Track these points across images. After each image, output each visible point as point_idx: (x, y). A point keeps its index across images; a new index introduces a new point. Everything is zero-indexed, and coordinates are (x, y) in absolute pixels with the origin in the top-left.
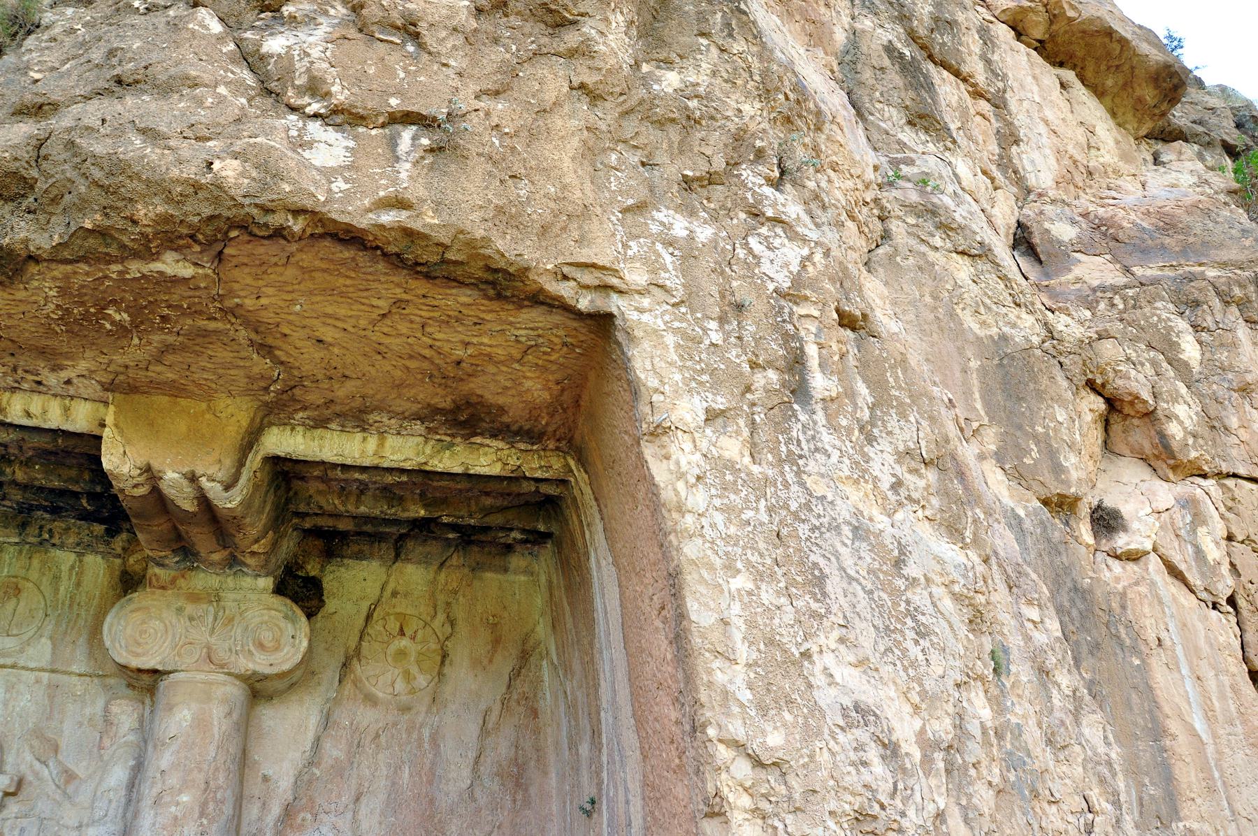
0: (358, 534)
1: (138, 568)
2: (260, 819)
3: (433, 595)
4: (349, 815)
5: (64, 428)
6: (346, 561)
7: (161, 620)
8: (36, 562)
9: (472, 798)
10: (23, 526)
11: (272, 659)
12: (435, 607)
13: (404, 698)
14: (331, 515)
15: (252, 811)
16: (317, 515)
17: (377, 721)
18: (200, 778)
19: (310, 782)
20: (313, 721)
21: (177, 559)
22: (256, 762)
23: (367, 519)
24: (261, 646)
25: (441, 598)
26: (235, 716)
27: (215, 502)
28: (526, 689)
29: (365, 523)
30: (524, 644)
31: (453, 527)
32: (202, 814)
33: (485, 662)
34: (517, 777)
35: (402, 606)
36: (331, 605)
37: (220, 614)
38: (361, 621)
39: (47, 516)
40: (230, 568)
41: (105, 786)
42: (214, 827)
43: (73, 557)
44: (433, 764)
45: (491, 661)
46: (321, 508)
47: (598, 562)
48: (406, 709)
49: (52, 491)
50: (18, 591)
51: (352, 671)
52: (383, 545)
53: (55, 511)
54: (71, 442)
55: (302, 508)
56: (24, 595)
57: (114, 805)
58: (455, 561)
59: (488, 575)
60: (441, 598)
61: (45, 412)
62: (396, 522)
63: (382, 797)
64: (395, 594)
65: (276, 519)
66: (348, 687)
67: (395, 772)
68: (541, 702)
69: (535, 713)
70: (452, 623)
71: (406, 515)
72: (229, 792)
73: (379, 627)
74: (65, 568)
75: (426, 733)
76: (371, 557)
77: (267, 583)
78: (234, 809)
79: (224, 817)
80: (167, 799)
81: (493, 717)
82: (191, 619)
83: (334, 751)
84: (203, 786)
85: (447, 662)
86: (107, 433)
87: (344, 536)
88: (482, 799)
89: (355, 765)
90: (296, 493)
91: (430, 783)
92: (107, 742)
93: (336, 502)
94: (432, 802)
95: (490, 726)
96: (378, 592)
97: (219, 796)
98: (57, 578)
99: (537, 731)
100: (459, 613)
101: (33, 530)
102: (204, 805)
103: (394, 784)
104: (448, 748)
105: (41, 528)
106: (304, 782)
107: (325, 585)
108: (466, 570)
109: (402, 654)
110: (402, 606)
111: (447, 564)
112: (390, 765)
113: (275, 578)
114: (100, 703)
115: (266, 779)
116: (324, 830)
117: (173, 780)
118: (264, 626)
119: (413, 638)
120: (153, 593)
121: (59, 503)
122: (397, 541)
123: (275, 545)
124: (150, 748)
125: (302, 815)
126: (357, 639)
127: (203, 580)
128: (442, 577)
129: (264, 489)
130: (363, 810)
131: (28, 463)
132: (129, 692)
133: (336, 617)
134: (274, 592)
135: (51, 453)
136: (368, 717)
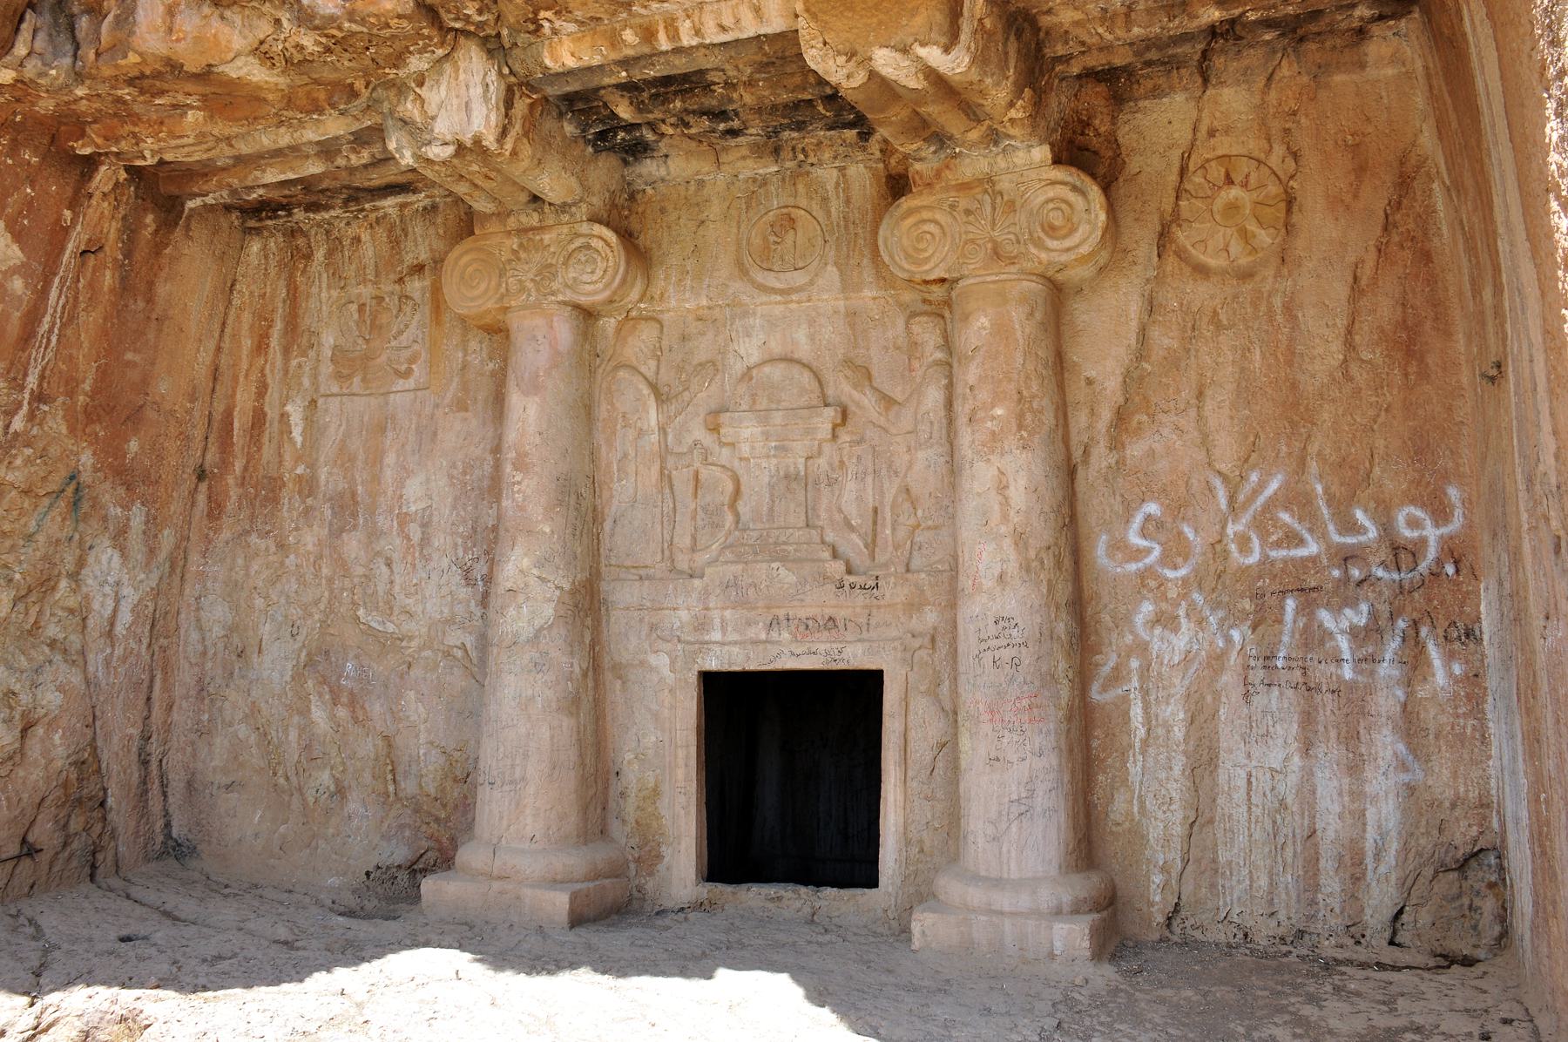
0: (1149, 64)
1: (900, 169)
2: (1090, 427)
3: (1263, 123)
4: (1193, 413)
5: (762, 32)
6: (1141, 104)
7: (936, 222)
8: (800, 187)
9: (1348, 377)
10: (777, 151)
11: (1067, 243)
13: (1244, 261)
14: (1101, 49)
15: (1079, 420)
16: (1083, 53)
18: (1011, 388)
19: (1141, 378)
20: (1135, 308)
21: (933, 149)
22: (1075, 364)
23: (1149, 43)
24: (1051, 230)
26: (1038, 316)
27: (941, 70)
28: (1411, 226)
29: (1148, 48)
30: (1402, 163)
31: (1268, 24)
32: (1020, 427)
33: (1348, 198)
34: (1408, 344)
36: (1134, 165)
37: (999, 200)
38: (1173, 178)
39: (795, 135)
40: (996, 143)
41: (923, 409)
42: (1037, 438)
43: (835, 173)
44: (1291, 339)
45: (1356, 196)
46: (1083, 43)
47: (1472, 20)
48: (1246, 275)
49: (786, 106)
50: (792, 220)
51: (1172, 241)
52: (1183, 71)
53: (800, 126)
54: (778, 46)
55: (1060, 50)
56: (799, 224)
57: (936, 427)
58: (1285, 71)
59: (1339, 78)
60: (1276, 126)
61: (738, 21)
62: (1186, 38)
63: (1231, 387)
64: (1212, 133)
65: (1031, 71)
66: (1171, 262)
67: (1243, 356)
68: (1436, 240)
69: (1426, 257)
70: (1296, 156)
71: (1196, 23)
72: (1046, 402)
73: (1198, 179)
74: (830, 187)
75: (1277, 302)
76: (1172, 88)
77: (1042, 153)
78: (1056, 418)
79: (1046, 428)
80: (981, 414)
81: (1367, 272)
82: (968, 212)
83: (1164, 340)
84: (1016, 397)
85: (1295, 208)
86: (801, 23)
87: (1128, 71)
88: (1360, 375)
89: (1193, 352)
90: (1047, 33)
91: (1290, 363)
92: (916, 364)
93: (1100, 30)
94: (1294, 386)
95: (1363, 282)
97: (1035, 405)
98: (825, 200)
99: (1432, 281)
100: (1304, 142)
101: (786, 153)
102: (1020, 417)
103: (1243, 370)
104: (1309, 318)
105: (794, 149)
106: (1132, 380)
107: (1121, 140)
109: (1233, 208)
110: (1223, 145)
111: (1276, 77)
112: (1234, 348)
113: (1052, 145)
114: (901, 322)
115: (1089, 382)
116: (1165, 432)
117: (984, 395)
118: (1051, 205)
119: (1245, 185)
120: (921, 193)
121: (796, 114)
122: (1200, 63)
123: (1038, 104)
124: (955, 365)
125: (1137, 418)
126: (1172, 199)
127: (975, 163)
128: (1273, 96)
129: (999, 37)
130: (1209, 405)
131: (750, 84)
132: (926, 308)
133: (1142, 177)
134: (1057, 161)
135: (767, 64)
136: (1201, 294)
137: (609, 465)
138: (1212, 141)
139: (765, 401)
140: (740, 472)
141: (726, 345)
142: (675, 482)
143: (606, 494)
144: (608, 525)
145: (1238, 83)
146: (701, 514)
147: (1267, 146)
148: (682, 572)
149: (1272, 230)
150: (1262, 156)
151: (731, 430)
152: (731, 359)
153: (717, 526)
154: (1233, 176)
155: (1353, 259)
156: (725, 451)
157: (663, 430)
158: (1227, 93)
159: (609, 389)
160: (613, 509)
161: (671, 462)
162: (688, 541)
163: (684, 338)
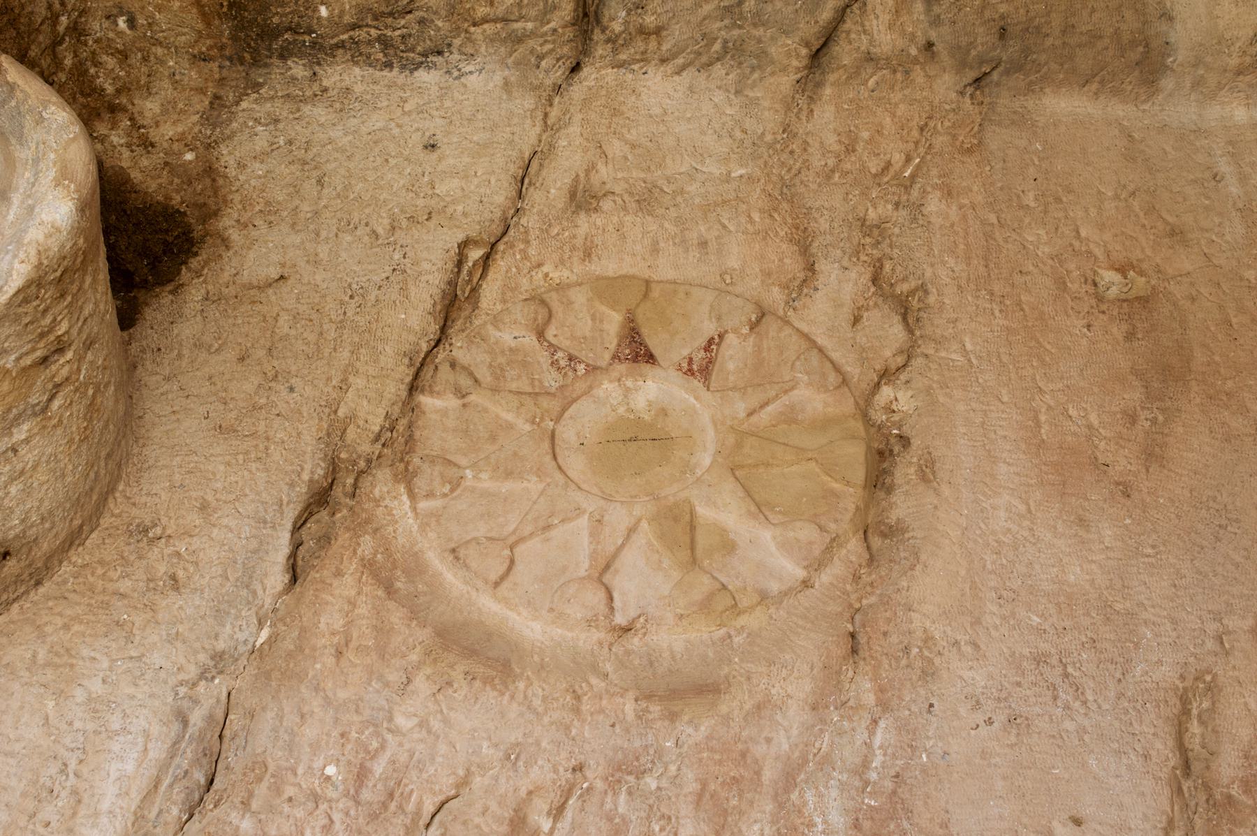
3: (785, 195)
6: (338, 74)
12: (803, 243)
17: (512, 757)
25: (830, 208)
33: (1124, 461)
35: (627, 246)
38: (413, 317)
45: (1153, 455)
59: (1062, 105)
64: (583, 198)
66: (341, 597)
73: (513, 334)
85: (904, 471)
96: (500, 195)
108: (945, 85)
109: (643, 440)
110: (627, 246)
111: (844, 52)
119: (701, 369)
126: (395, 389)
128: (825, 122)
138: (584, 224)
145: (701, 56)
147: (793, 265)
149: (805, 532)
150: (776, 297)
154: (654, 343)
155: (1167, 673)
158: (658, 91)
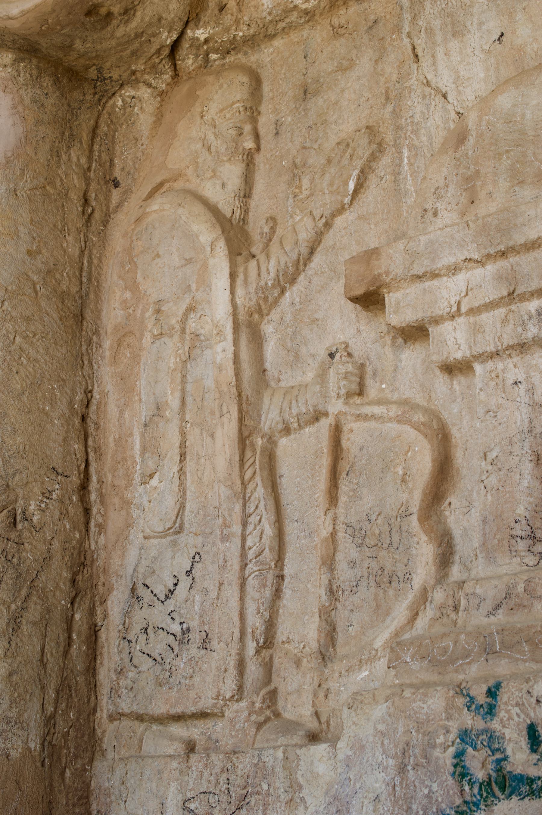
137: (121, 443)
139: (503, 184)
140: (453, 413)
141: (403, 77)
142: (287, 469)
143: (115, 520)
144: (116, 603)
146: (347, 550)
148: (291, 727)
151: (414, 290)
152: (415, 105)
153: (389, 580)
156: (411, 357)
157: (248, 327)
159: (129, 250)
160: (132, 554)
161: (270, 416)
162: (311, 631)
163: (306, 93)
